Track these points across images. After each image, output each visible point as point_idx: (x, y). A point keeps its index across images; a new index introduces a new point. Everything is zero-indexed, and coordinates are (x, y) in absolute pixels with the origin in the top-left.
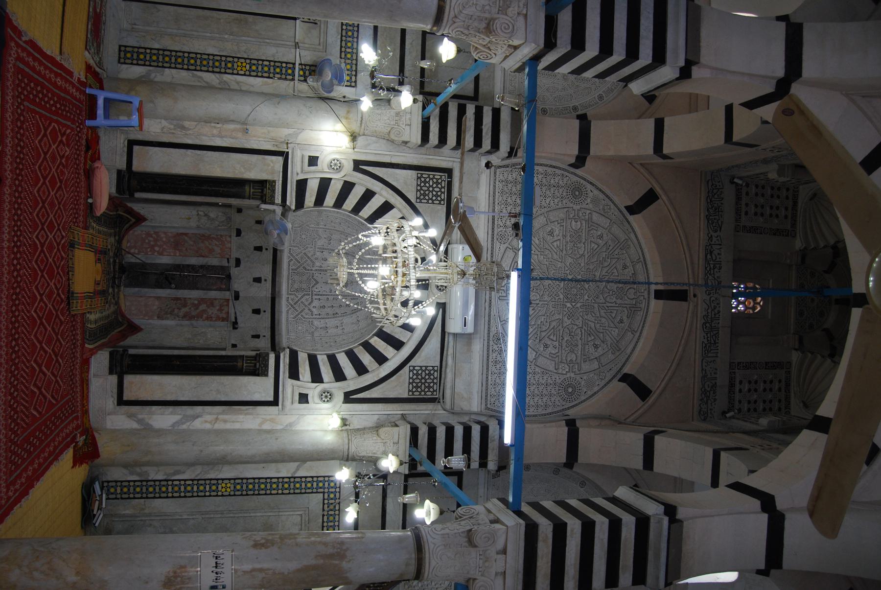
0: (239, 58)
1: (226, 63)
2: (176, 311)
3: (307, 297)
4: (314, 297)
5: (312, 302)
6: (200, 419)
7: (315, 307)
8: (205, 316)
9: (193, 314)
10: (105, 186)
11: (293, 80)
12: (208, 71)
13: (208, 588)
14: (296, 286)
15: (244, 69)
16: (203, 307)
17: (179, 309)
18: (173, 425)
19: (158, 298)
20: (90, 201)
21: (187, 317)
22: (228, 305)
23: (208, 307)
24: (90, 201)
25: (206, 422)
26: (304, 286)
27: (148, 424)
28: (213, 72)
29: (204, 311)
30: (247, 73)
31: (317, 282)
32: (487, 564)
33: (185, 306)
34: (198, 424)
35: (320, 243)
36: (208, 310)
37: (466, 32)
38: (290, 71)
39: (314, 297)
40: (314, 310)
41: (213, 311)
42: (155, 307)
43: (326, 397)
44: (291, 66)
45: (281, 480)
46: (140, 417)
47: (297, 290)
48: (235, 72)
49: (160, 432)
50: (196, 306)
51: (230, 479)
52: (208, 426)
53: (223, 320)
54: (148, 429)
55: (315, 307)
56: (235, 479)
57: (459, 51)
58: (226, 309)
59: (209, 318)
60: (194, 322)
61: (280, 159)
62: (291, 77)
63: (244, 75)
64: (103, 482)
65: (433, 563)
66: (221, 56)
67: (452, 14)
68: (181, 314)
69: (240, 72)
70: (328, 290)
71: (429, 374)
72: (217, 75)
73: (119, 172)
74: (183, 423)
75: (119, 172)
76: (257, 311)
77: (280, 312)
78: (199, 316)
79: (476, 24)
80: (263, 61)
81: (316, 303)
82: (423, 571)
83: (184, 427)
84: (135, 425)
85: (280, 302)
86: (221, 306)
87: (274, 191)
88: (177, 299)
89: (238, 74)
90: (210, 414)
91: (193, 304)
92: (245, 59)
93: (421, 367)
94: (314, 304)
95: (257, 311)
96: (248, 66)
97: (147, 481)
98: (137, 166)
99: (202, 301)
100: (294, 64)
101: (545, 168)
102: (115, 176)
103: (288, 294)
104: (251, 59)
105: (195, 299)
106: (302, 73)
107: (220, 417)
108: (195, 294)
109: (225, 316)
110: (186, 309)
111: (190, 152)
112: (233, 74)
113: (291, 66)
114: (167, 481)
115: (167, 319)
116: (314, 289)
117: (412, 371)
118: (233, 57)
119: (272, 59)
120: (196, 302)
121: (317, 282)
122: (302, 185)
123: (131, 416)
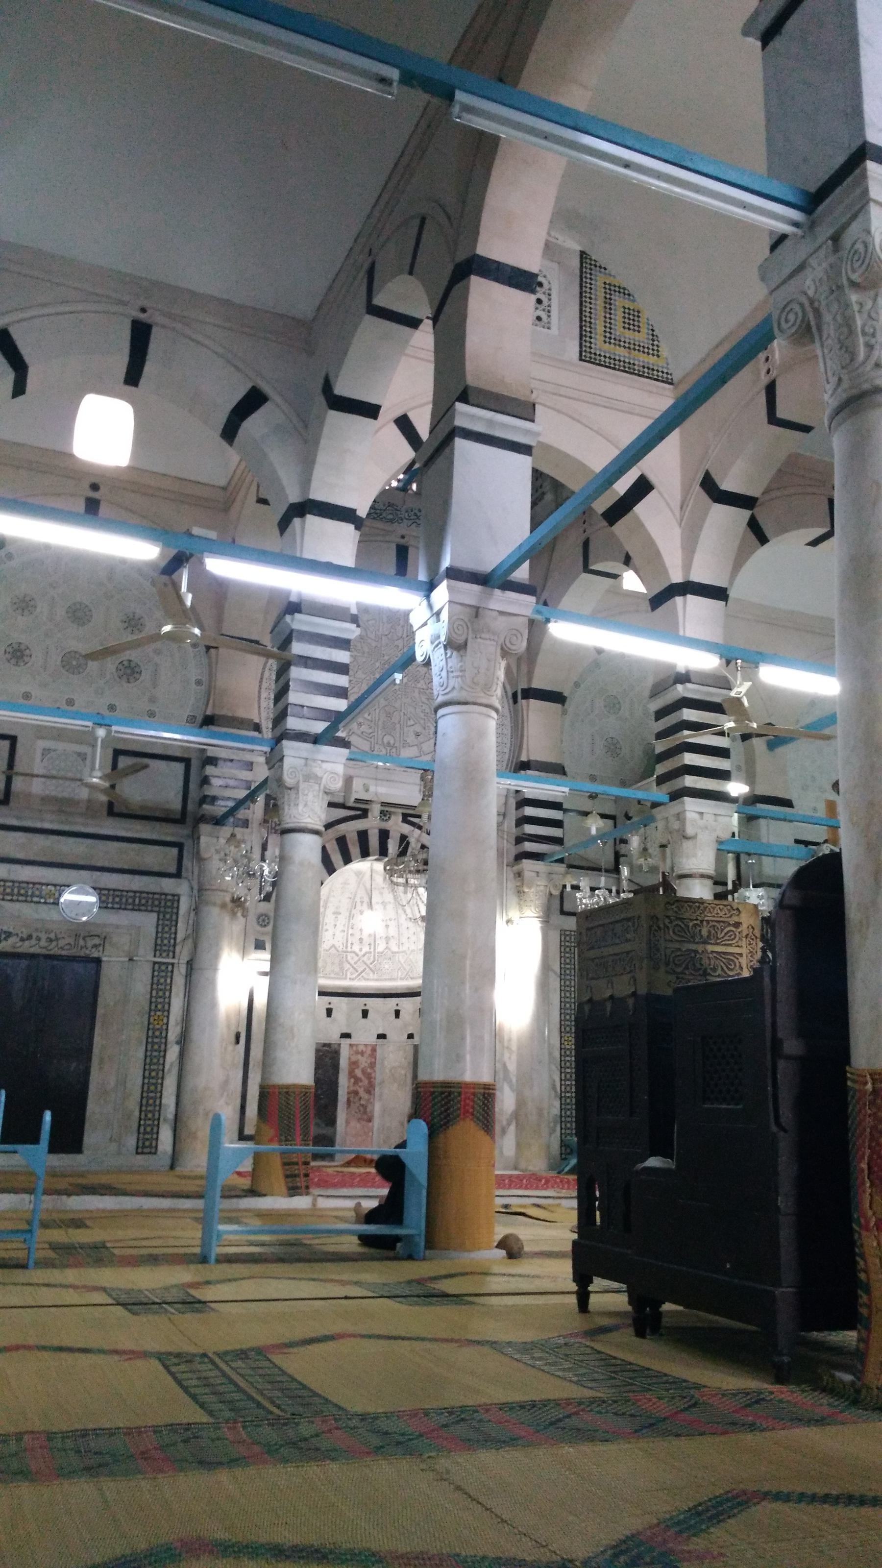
0: (149, 1024)
1: (154, 1036)
2: (362, 1102)
3: (349, 958)
4: (349, 949)
5: (354, 952)
6: (508, 1065)
7: (361, 950)
8: (369, 1070)
9: (366, 1082)
11: (173, 964)
12: (164, 1056)
14: (337, 970)
15: (161, 1018)
16: (358, 1073)
17: (360, 1098)
18: (513, 1090)
19: (347, 1122)
21: (370, 1090)
22: (357, 1045)
23: (358, 1067)
25: (510, 1058)
26: (337, 961)
27: (511, 1115)
28: (165, 1051)
29: (364, 1072)
30: (166, 1014)
31: (333, 946)
33: (356, 1093)
34: (512, 1067)
36: (362, 1066)
38: (163, 968)
39: (349, 949)
40: (364, 951)
41: (364, 1061)
42: (358, 1126)
44: (157, 967)
45: (563, 988)
46: (505, 1123)
47: (342, 969)
48: (165, 1027)
49: (521, 1103)
50: (357, 1080)
51: (561, 1037)
52: (514, 1057)
53: (374, 1050)
54: (516, 1115)
55: (361, 950)
56: (561, 1032)
58: (361, 1048)
59: (373, 1065)
60: (377, 1081)
62: (170, 968)
63: (168, 1017)
64: (562, 1159)
66: (147, 1042)
68: (366, 1096)
69: (165, 1021)
70: (342, 934)
72: (169, 1046)
74: (511, 1081)
76: (365, 1014)
77: (367, 988)
78: (369, 1077)
80: (151, 997)
81: (356, 948)
83: (514, 1080)
84: (513, 1128)
85: (357, 988)
86: (357, 1053)
88: (349, 1102)
89: (167, 1024)
90: (503, 1055)
91: (355, 1083)
92: (150, 1016)
94: (357, 951)
95: (365, 1014)
96: (158, 1013)
97: (561, 1116)
99: (351, 1074)
100: (155, 963)
101: (263, 690)
103: (345, 979)
104: (150, 1010)
105: (349, 1081)
106: (164, 954)
107: (506, 1044)
108: (343, 1081)
109: (369, 1048)
110: (362, 1093)
112: (167, 1029)
113: (157, 967)
114: (561, 1098)
115: (372, 1111)
116: (340, 949)
118: (149, 1029)
119: (149, 987)
120: (352, 1080)
121: (333, 946)
123: (504, 1131)
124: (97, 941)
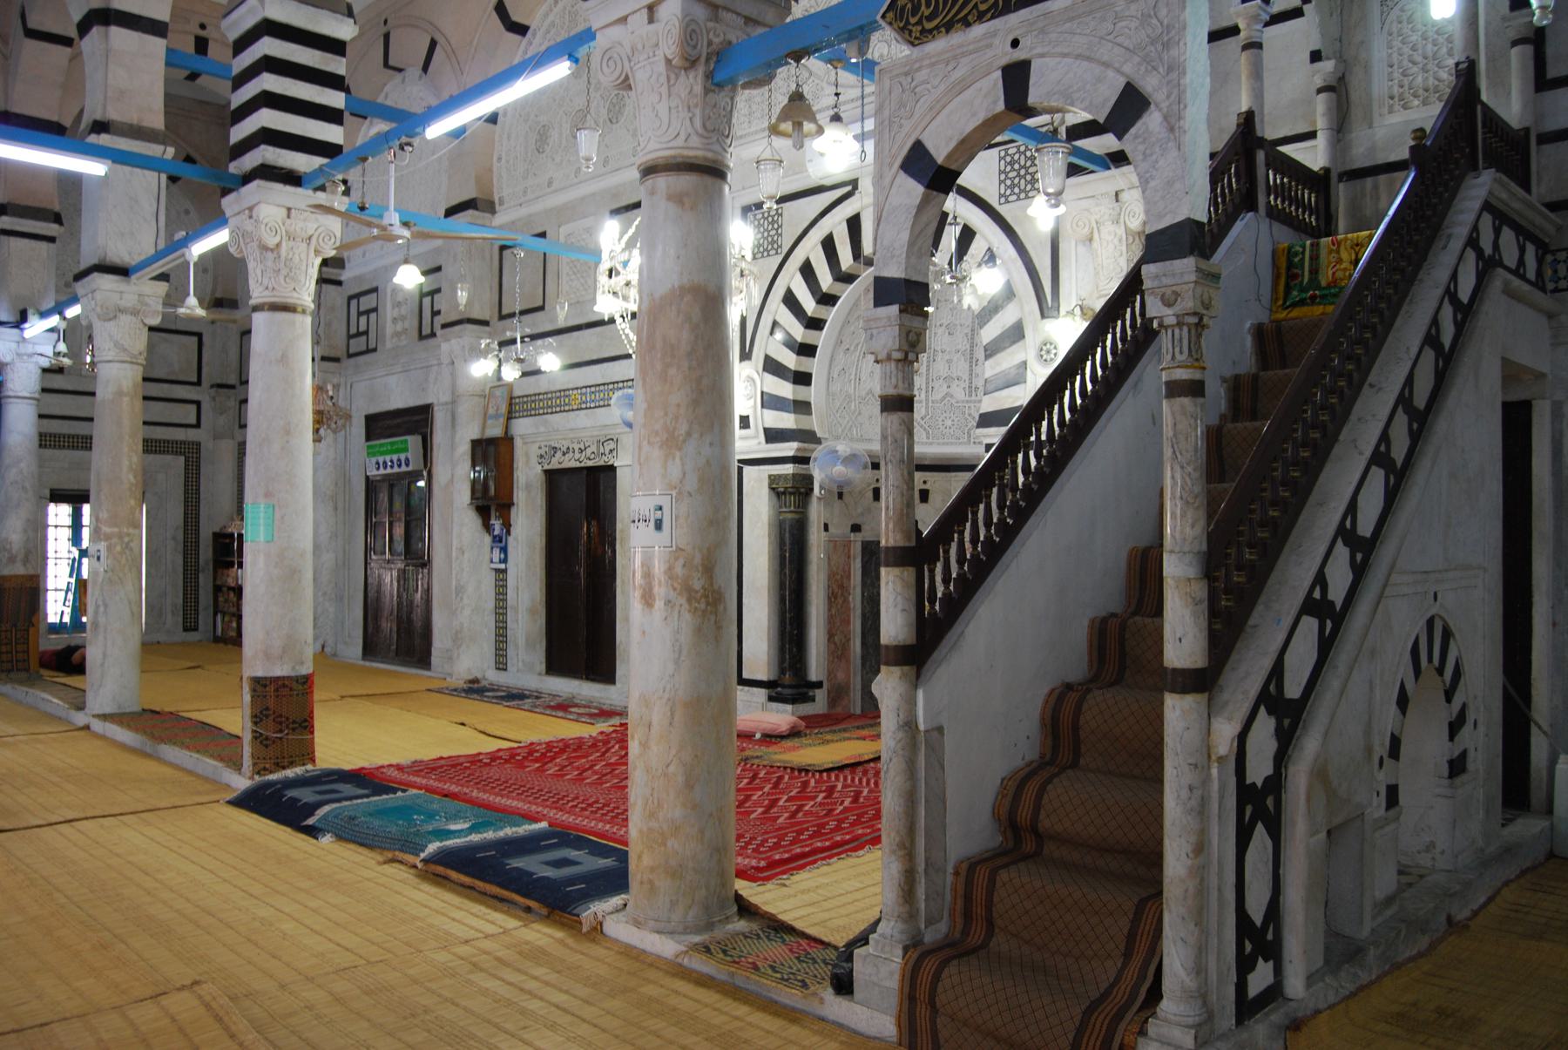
10: (781, 717)
13: (657, 534)
20: (758, 736)
24: (758, 736)
32: (640, 47)
35: (959, 392)
37: (284, 272)
43: (1048, 352)
57: (406, 262)
61: (747, 469)
65: (653, 145)
67: (267, 293)
71: (1011, 163)
73: (771, 699)
75: (771, 699)
79: (270, 263)
82: (661, 162)
87: (780, 476)
93: (1001, 182)
98: (762, 675)
102: (774, 705)
111: (745, 600)
117: (1006, 197)
122: (773, 435)
124: (612, 445)
